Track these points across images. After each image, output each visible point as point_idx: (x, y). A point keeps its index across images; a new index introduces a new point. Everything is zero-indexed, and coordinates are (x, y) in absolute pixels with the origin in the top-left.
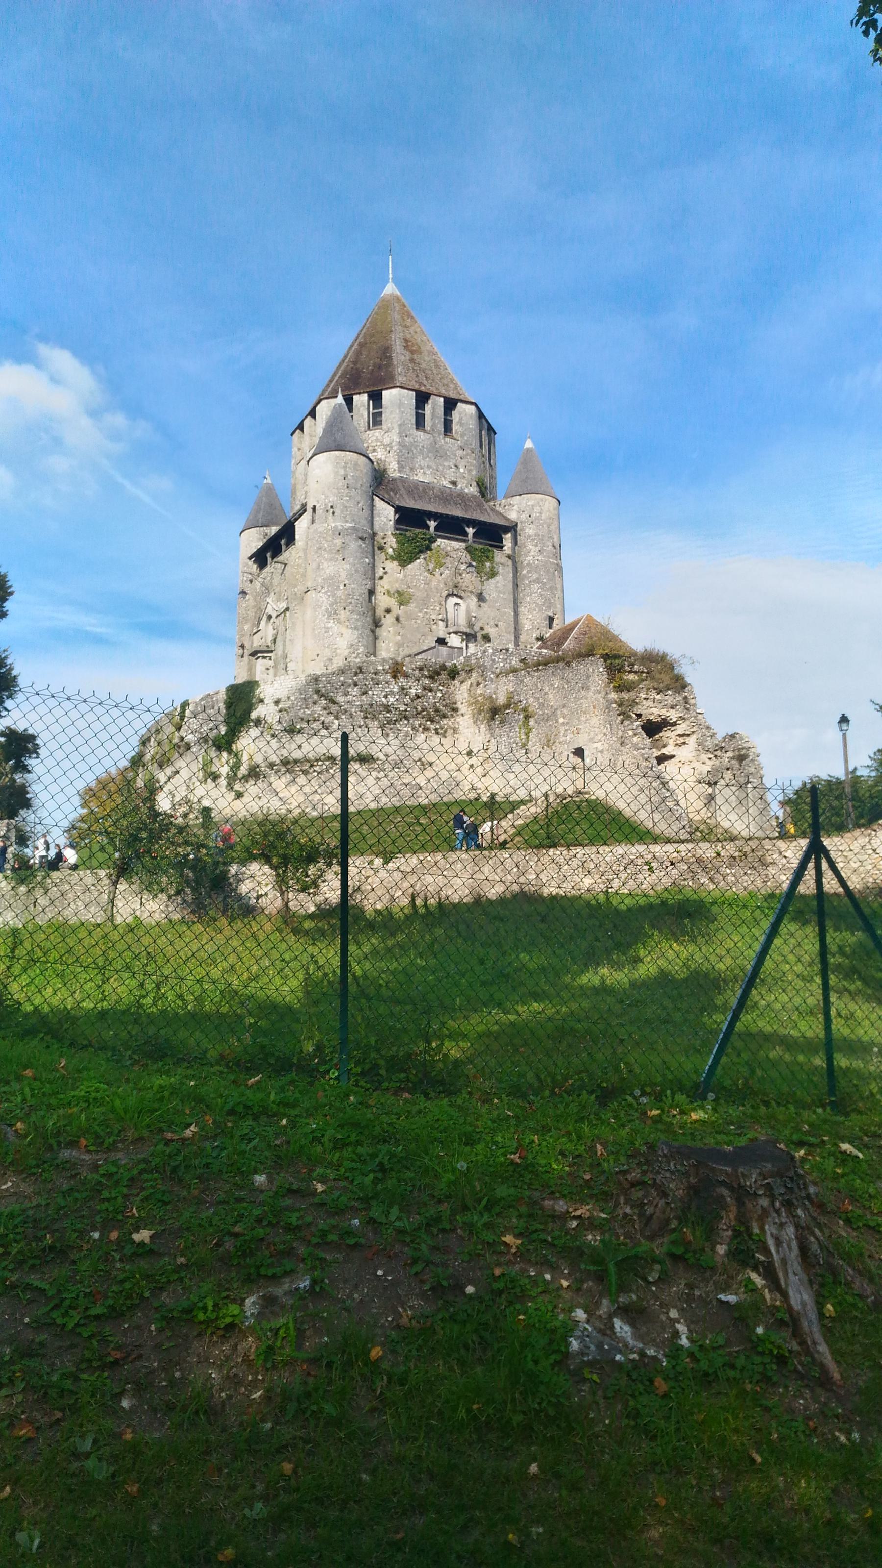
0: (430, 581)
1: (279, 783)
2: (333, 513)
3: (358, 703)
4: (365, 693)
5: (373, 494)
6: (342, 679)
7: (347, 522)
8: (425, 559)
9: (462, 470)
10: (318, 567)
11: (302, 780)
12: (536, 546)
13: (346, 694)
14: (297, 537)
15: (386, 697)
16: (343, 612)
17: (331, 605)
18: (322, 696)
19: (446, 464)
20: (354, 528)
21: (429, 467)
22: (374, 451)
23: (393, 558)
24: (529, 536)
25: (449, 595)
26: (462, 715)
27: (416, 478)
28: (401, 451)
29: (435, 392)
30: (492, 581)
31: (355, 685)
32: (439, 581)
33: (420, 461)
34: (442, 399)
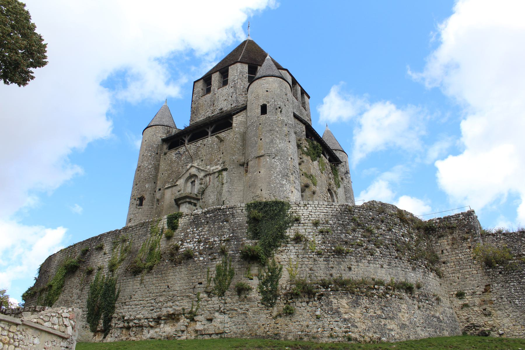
1: (343, 303)
2: (281, 111)
3: (388, 237)
4: (390, 230)
6: (371, 213)
10: (272, 141)
11: (364, 301)
13: (378, 228)
14: (234, 125)
15: (403, 236)
16: (291, 176)
17: (284, 169)
18: (359, 225)
23: (308, 154)
26: (444, 263)
31: (382, 222)
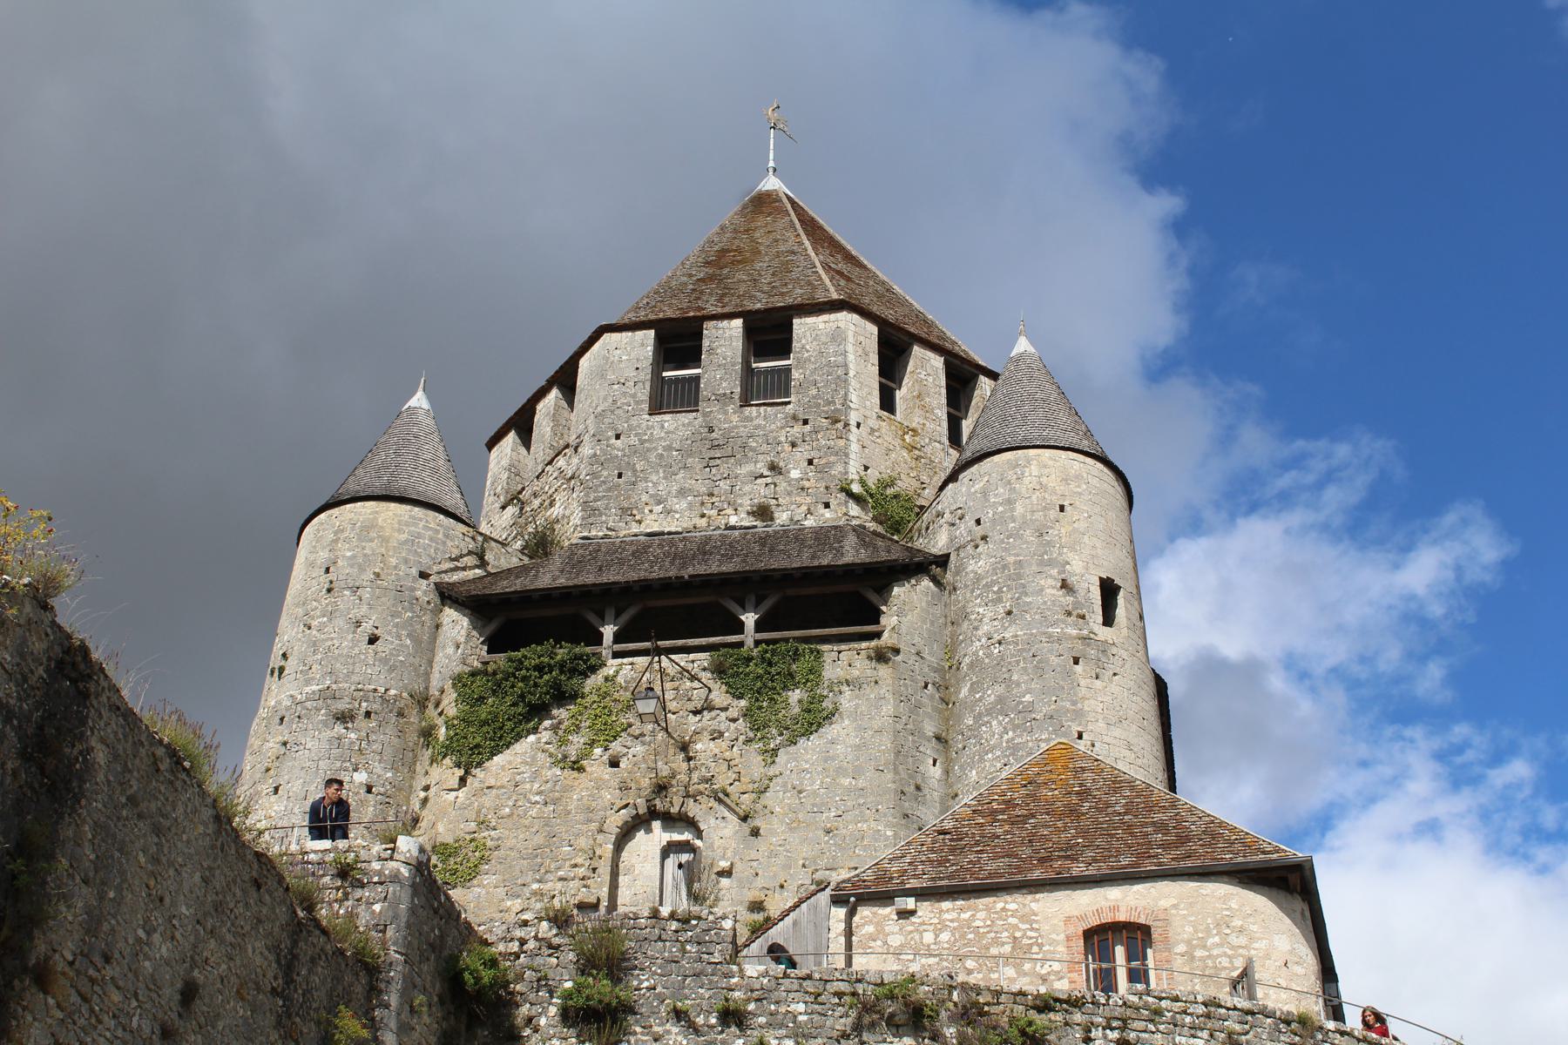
0: (567, 789)
5: (447, 595)
7: (308, 682)
8: (555, 728)
9: (795, 474)
12: (1000, 600)
19: (743, 470)
20: (327, 695)
21: (682, 493)
22: (552, 504)
24: (978, 579)
25: (638, 823)
27: (635, 528)
28: (594, 475)
29: (711, 309)
30: (811, 746)
32: (599, 785)
33: (656, 483)
34: (738, 323)
